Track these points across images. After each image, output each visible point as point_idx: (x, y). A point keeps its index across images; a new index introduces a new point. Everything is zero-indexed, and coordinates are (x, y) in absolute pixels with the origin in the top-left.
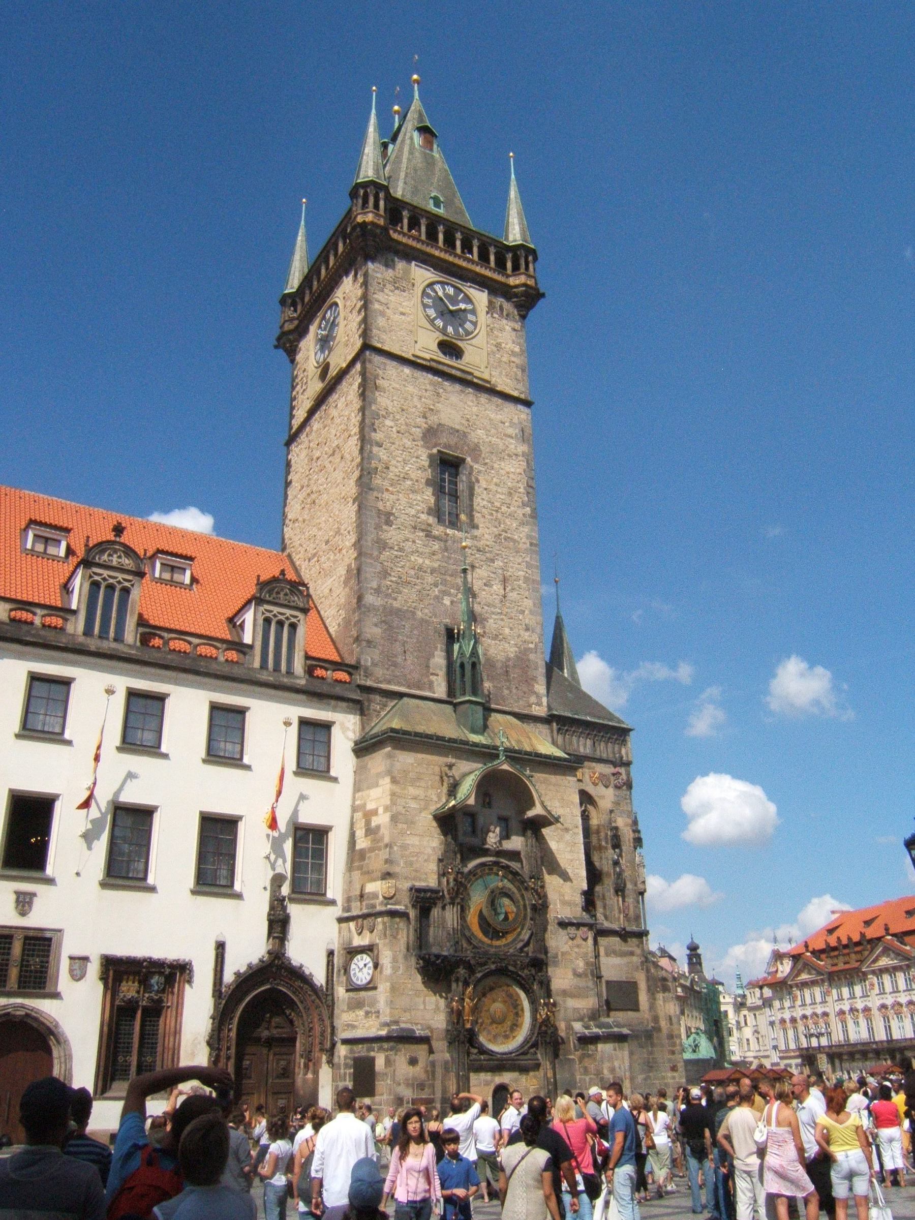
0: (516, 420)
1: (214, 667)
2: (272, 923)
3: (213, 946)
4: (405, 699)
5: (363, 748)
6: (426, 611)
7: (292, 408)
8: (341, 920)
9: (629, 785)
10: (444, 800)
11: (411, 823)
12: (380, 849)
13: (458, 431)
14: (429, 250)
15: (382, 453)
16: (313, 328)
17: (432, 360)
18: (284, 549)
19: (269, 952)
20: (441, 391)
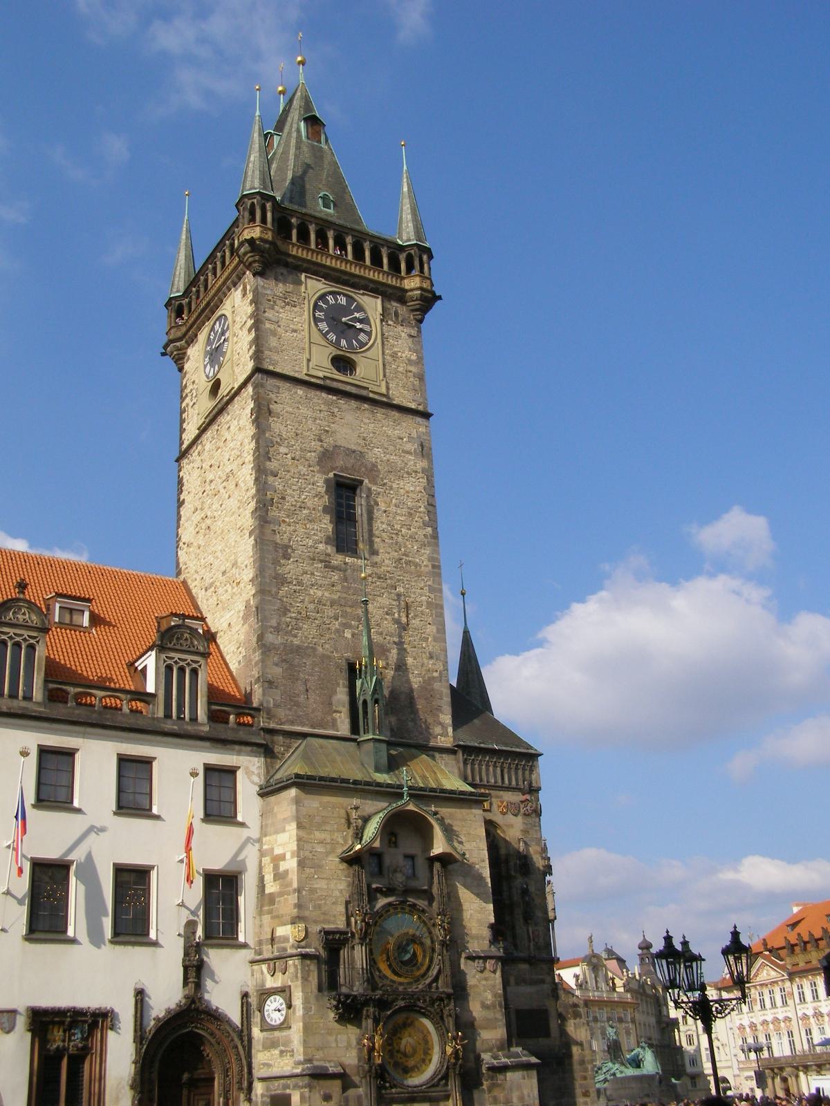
0: (414, 435)
1: (120, 720)
3: (132, 993)
4: (309, 738)
5: (267, 792)
6: (327, 646)
7: (182, 421)
8: (253, 962)
9: (537, 812)
10: (350, 843)
11: (318, 867)
12: (288, 894)
13: (354, 452)
14: (319, 259)
15: (277, 483)
16: (202, 337)
17: (325, 378)
18: (179, 573)
19: (186, 997)
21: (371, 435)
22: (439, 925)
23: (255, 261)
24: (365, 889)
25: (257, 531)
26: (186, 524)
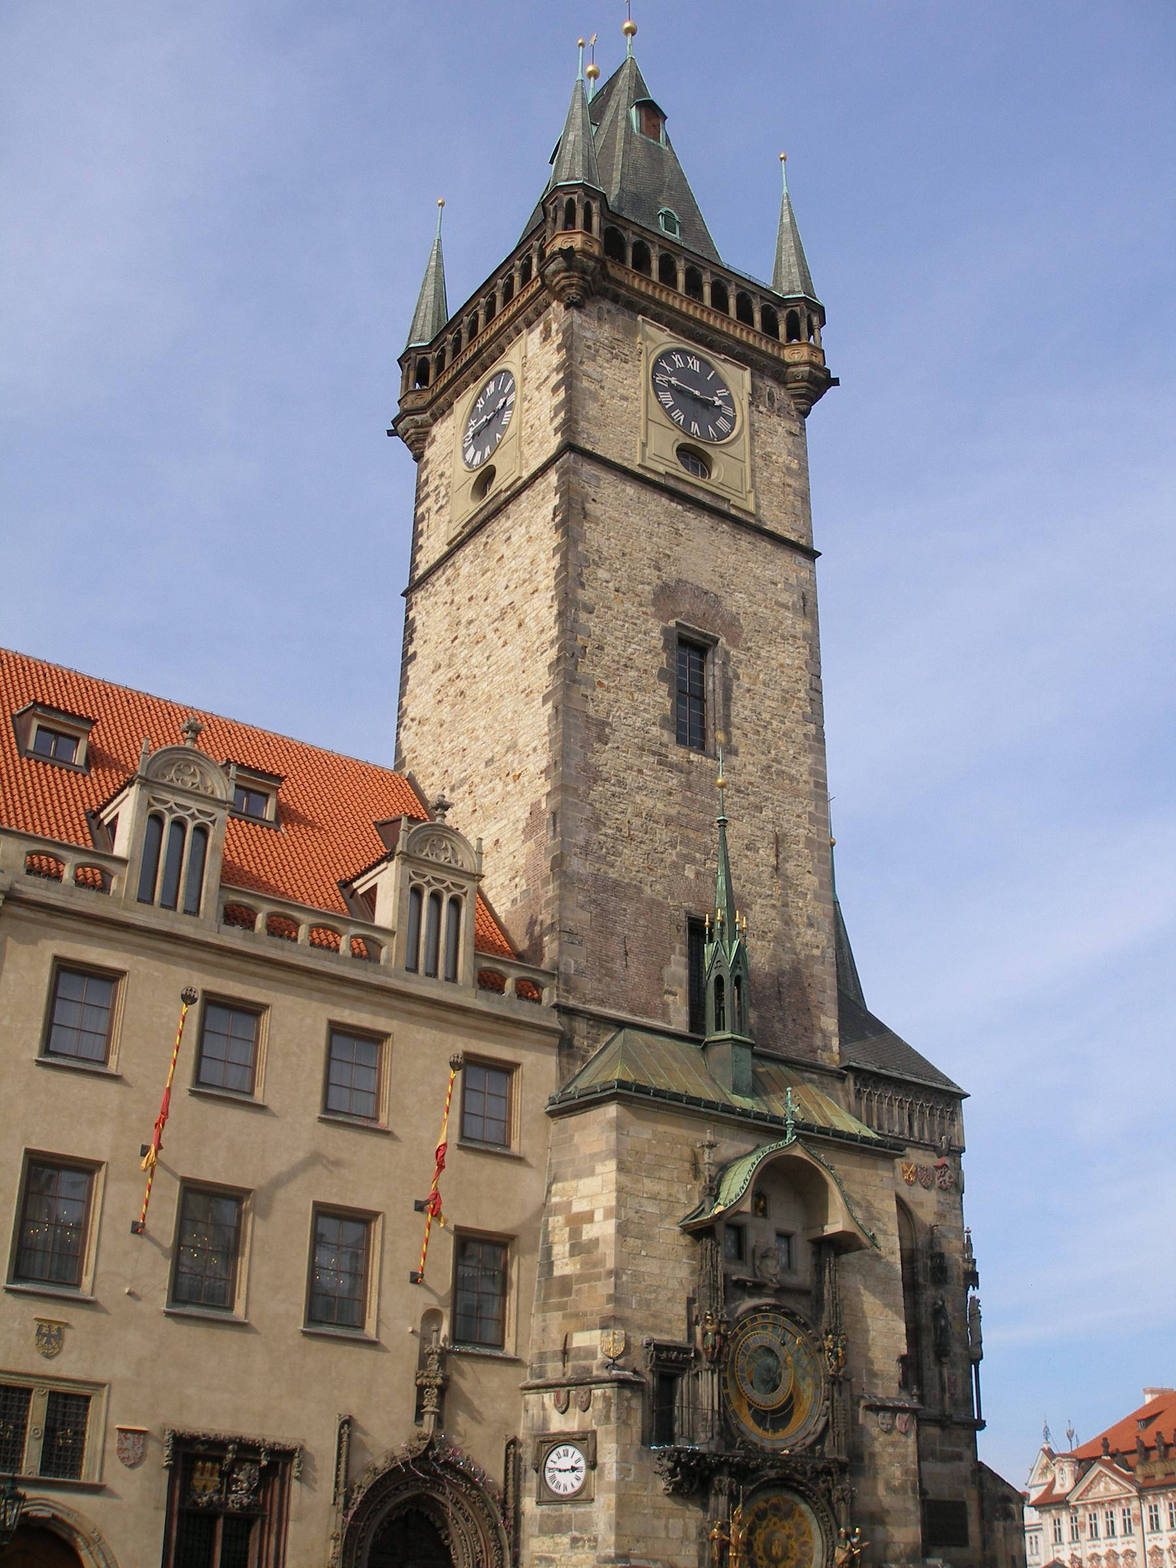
0: (793, 581)
2: (421, 1389)
4: (627, 1030)
6: (658, 887)
7: (417, 534)
10: (697, 1202)
11: (646, 1237)
12: (598, 1278)
13: (706, 593)
15: (593, 623)
16: (462, 406)
20: (681, 526)
21: (732, 571)
22: (830, 1350)
23: (571, 285)
24: (720, 1280)
25: (559, 694)
26: (418, 691)
